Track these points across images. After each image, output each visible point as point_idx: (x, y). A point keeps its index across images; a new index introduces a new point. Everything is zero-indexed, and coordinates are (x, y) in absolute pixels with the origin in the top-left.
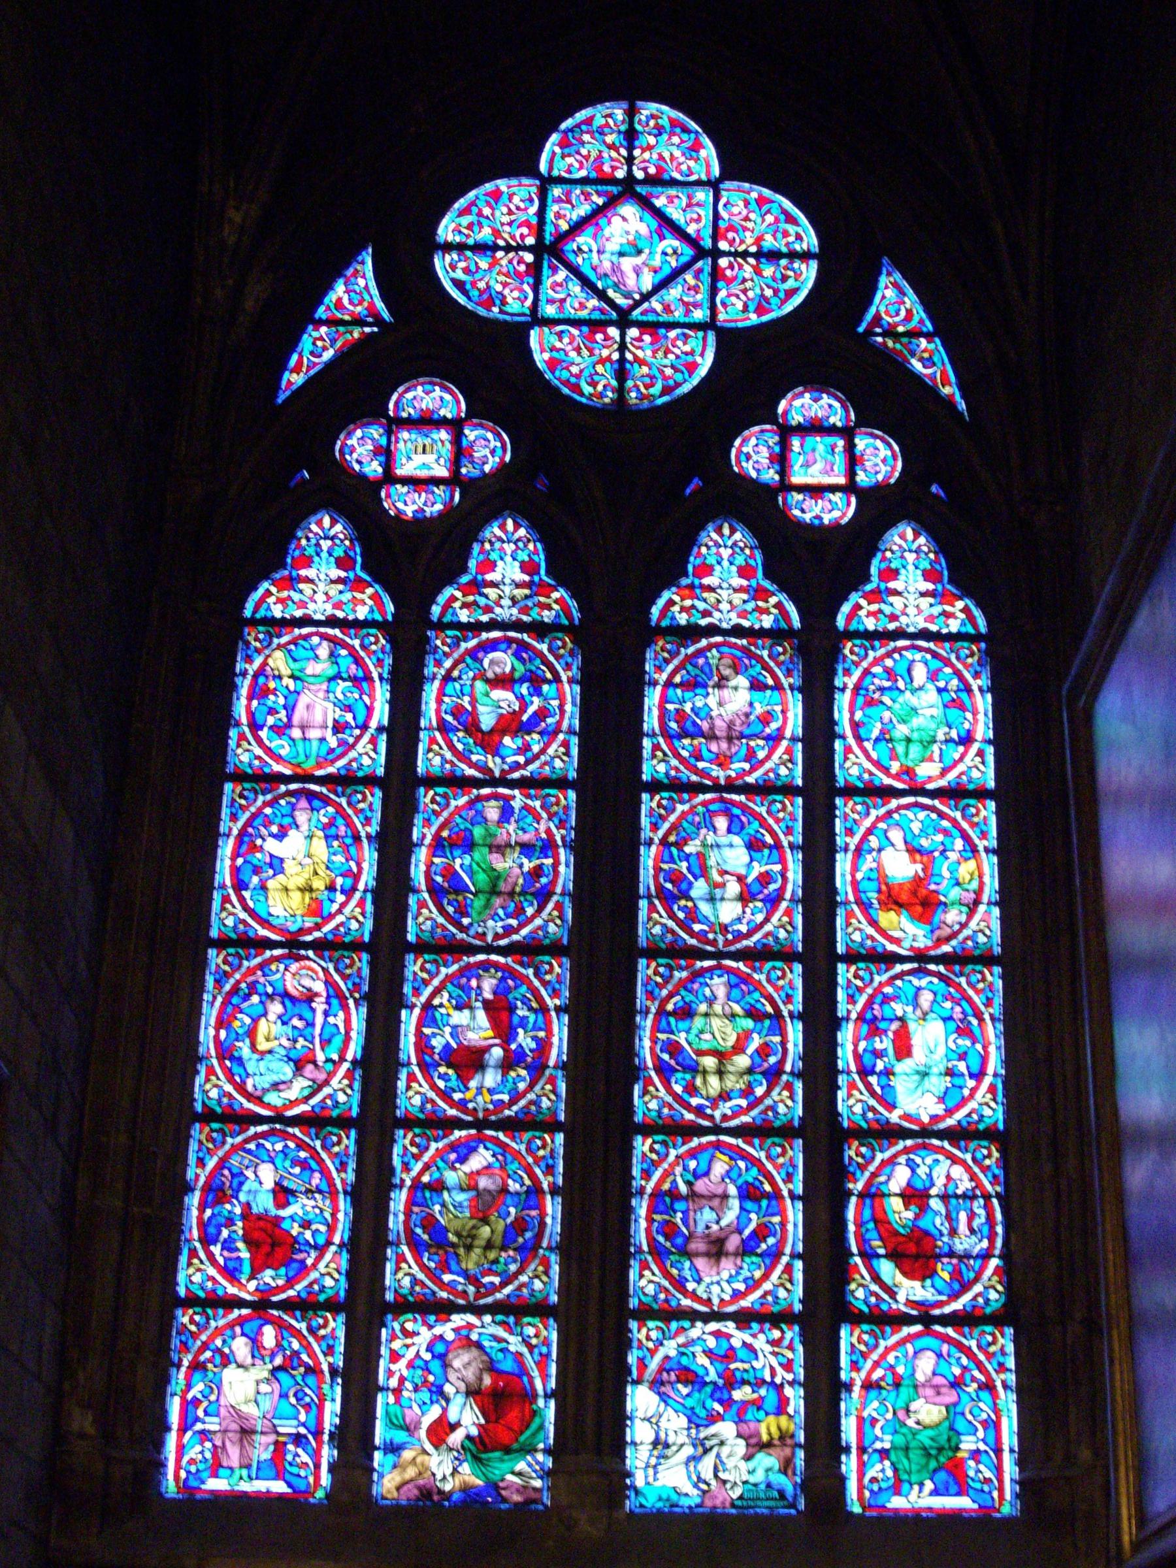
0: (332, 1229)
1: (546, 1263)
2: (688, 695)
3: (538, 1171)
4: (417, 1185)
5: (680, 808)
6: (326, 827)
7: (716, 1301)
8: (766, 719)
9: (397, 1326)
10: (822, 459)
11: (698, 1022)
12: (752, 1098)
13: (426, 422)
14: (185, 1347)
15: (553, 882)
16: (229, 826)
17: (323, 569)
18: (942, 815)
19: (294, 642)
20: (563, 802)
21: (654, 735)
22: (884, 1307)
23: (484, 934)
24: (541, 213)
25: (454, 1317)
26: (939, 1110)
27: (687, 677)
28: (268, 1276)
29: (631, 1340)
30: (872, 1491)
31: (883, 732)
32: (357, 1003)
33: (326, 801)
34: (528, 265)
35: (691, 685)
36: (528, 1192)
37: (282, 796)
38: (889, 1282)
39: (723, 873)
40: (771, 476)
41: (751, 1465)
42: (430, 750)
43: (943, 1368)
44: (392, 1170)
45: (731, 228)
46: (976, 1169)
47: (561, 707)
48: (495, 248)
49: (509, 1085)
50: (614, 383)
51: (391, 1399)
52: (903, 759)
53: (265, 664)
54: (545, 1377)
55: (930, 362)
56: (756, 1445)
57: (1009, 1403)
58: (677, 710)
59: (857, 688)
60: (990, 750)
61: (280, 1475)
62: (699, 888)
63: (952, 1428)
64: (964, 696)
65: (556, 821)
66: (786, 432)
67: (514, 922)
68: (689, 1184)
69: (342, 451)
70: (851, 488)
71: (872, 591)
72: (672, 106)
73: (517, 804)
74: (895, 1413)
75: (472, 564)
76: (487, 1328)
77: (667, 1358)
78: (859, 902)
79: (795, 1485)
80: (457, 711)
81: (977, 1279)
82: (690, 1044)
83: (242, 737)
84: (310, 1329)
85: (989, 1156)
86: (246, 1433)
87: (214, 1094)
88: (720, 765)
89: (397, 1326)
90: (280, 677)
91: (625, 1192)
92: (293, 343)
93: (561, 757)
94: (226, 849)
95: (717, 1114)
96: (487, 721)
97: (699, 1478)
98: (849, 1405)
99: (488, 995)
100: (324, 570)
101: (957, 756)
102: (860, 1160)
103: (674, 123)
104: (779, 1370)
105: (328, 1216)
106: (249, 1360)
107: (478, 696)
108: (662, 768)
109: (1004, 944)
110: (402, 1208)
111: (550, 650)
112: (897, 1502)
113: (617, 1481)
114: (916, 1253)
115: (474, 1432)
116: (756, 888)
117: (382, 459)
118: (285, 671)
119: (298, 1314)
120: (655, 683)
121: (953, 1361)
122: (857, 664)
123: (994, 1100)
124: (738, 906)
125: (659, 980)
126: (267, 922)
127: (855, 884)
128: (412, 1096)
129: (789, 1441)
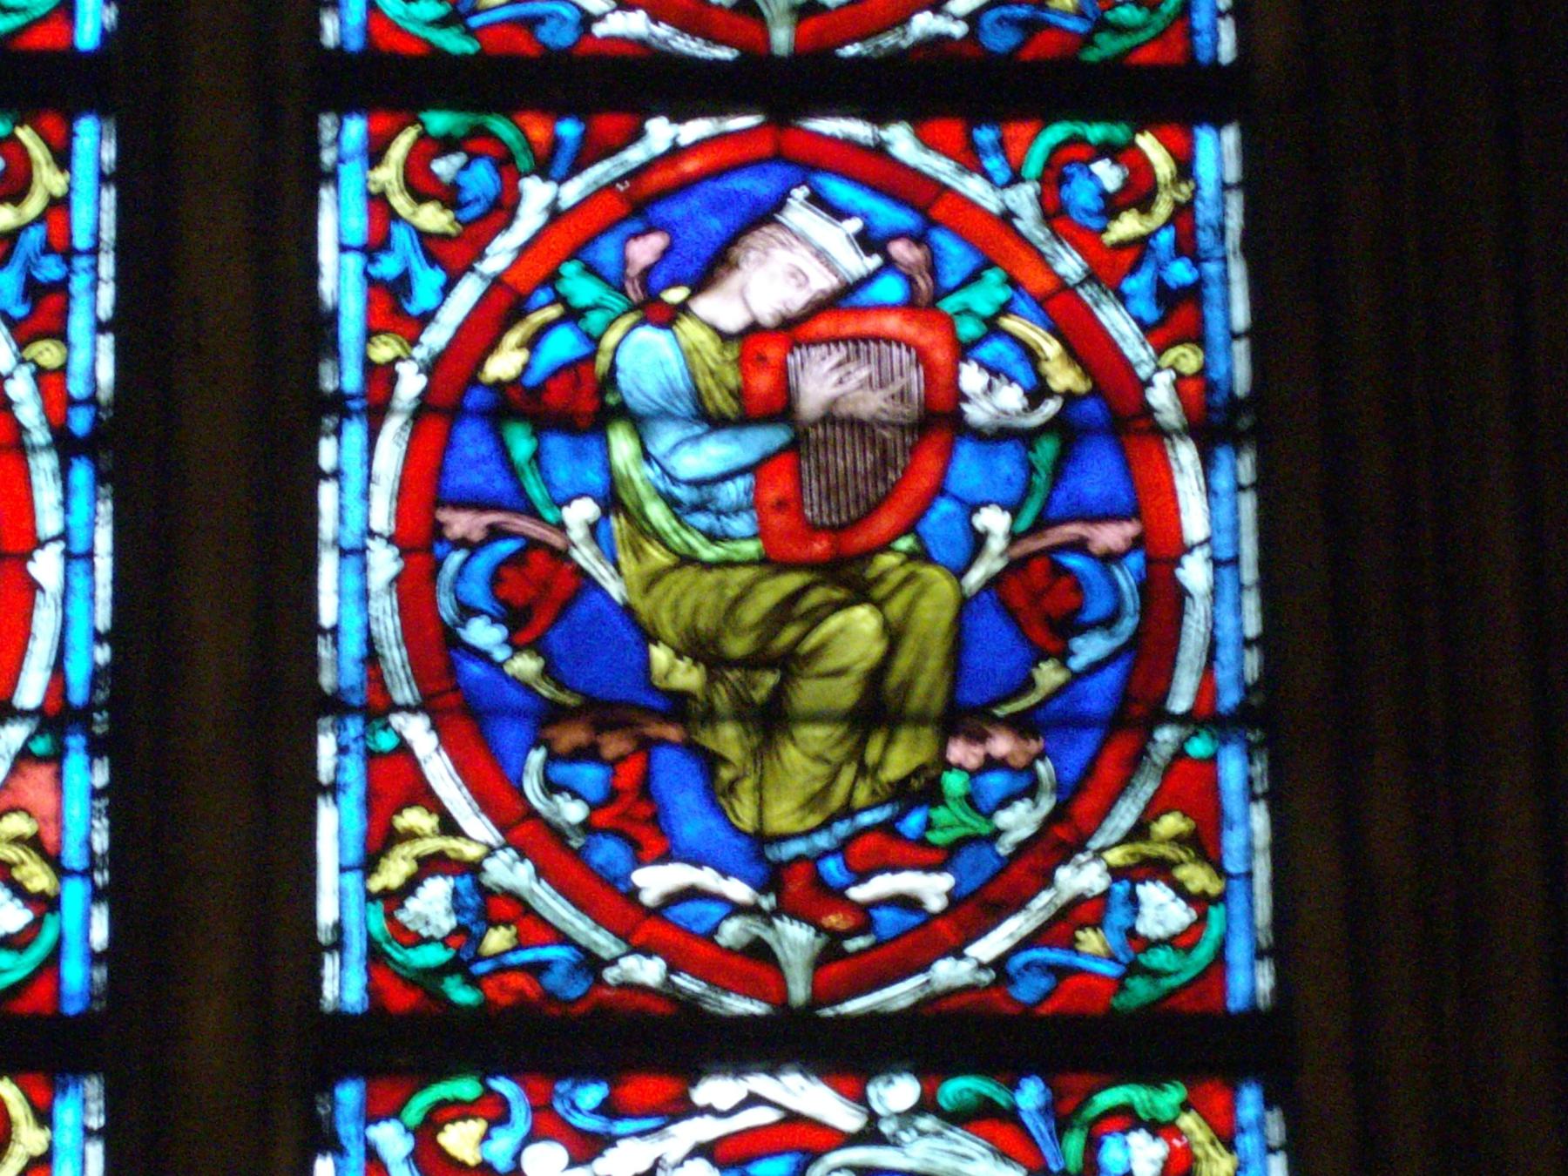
1: (1192, 789)
4: (455, 394)
9: (393, 1140)
25: (716, 1090)
44: (320, 328)
110: (382, 516)
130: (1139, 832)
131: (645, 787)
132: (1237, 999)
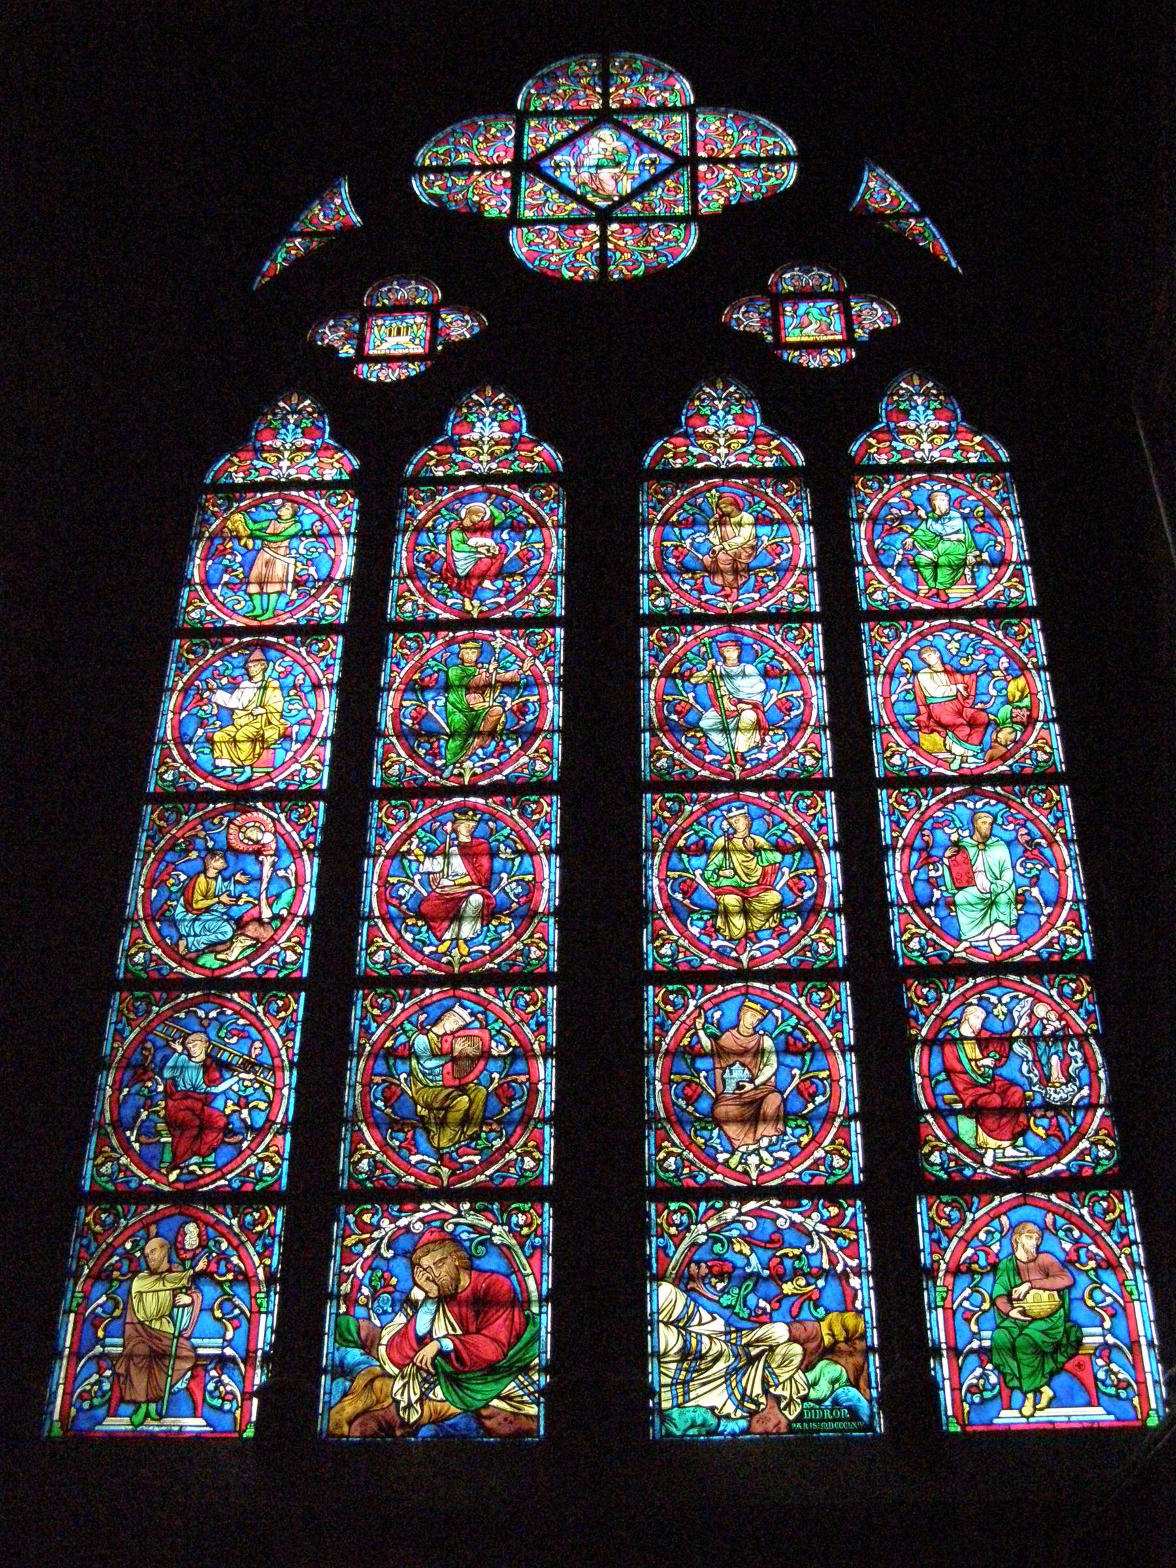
2: (686, 532)
3: (526, 1029)
7: (754, 1175)
8: (776, 549)
9: (351, 1218)
11: (718, 859)
12: (785, 938)
16: (175, 680)
18: (980, 634)
21: (653, 572)
22: (968, 1172)
23: (461, 775)
25: (425, 1206)
27: (684, 515)
29: (648, 1227)
30: (972, 1404)
33: (283, 651)
34: (505, 180)
36: (514, 1057)
37: (236, 648)
38: (971, 1142)
41: (811, 1376)
43: (1050, 1243)
44: (350, 1035)
49: (491, 935)
60: (1027, 571)
62: (710, 719)
63: (1067, 1318)
65: (543, 658)
68: (714, 1037)
73: (497, 644)
74: (993, 1303)
76: (465, 1219)
77: (694, 1245)
78: (895, 725)
79: (870, 1401)
81: (1080, 1135)
82: (707, 882)
88: (727, 596)
89: (351, 1218)
90: (239, 538)
94: (171, 703)
95: (744, 958)
96: (463, 565)
97: (744, 1395)
99: (464, 839)
104: (840, 1255)
105: (269, 1090)
106: (165, 1266)
108: (661, 602)
109: (1068, 761)
111: (532, 497)
112: (1008, 1418)
114: (1004, 1110)
116: (775, 715)
117: (355, 342)
120: (650, 524)
124: (757, 737)
126: (212, 774)
128: (379, 948)
129: (860, 1345)
130: (525, 1145)
131: (413, 1138)
132: (546, 1182)
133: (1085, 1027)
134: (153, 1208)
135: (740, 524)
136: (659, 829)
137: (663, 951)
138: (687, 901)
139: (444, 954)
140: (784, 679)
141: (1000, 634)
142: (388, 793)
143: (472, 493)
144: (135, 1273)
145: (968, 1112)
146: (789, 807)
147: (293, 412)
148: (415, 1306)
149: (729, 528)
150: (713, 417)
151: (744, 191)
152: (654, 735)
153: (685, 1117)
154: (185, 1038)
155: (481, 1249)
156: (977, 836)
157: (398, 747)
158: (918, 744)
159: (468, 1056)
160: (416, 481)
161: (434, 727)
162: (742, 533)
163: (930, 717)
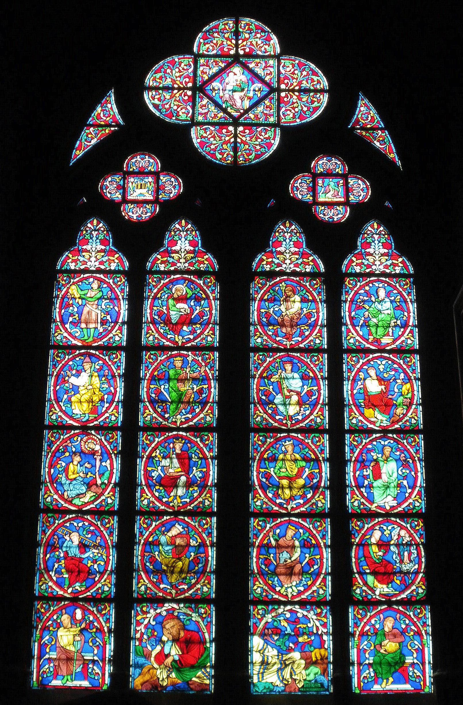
0: (107, 563)
2: (271, 305)
3: (204, 535)
5: (268, 360)
6: (99, 370)
8: (309, 316)
9: (139, 609)
10: (332, 190)
11: (279, 464)
12: (305, 499)
13: (141, 173)
14: (39, 619)
15: (209, 396)
17: (94, 245)
18: (394, 362)
19: (81, 281)
20: (212, 357)
22: (369, 597)
23: (176, 422)
24: (195, 71)
25: (166, 605)
26: (395, 503)
28: (77, 586)
29: (250, 614)
30: (364, 683)
31: (365, 322)
32: (116, 455)
34: (189, 97)
35: (272, 300)
36: (199, 546)
38: (372, 586)
39: (290, 391)
40: (309, 198)
41: (308, 672)
42: (147, 333)
45: (286, 78)
46: (412, 532)
47: (210, 311)
48: (173, 89)
50: (232, 153)
51: (137, 643)
52: (374, 335)
53: (67, 292)
54: (210, 633)
55: (383, 142)
56: (309, 663)
57: (428, 641)
58: (266, 312)
59: (352, 301)
61: (86, 678)
62: (279, 399)
64: (404, 305)
65: (209, 366)
66: (315, 176)
67: (190, 416)
68: (276, 540)
69: (101, 188)
70: (346, 203)
71: (358, 253)
72: (257, 20)
73: (190, 359)
74: (375, 647)
75: (166, 242)
77: (267, 623)
80: (160, 314)
81: (413, 583)
82: (276, 474)
83: (57, 327)
84: (98, 610)
85: (418, 525)
86: (69, 659)
87: (49, 500)
88: (287, 339)
89: (139, 609)
90: (75, 299)
91: (246, 545)
92: (77, 136)
93: (212, 337)
94: (51, 381)
95: (289, 507)
97: (283, 678)
98: (353, 643)
99: (178, 451)
100: (94, 245)
101: (400, 333)
102: (357, 528)
103: (257, 28)
104: (320, 627)
105: (104, 557)
106: (70, 626)
107: (170, 306)
108: (259, 340)
112: (376, 687)
113: (246, 680)
114: (384, 572)
115: (177, 658)
116: (306, 398)
117: (121, 191)
118: (77, 296)
119: (92, 604)
121: (402, 622)
122: (352, 289)
123: (420, 498)
124: (298, 408)
125: (260, 443)
127: (352, 395)
128: (145, 499)
130: (204, 582)
131: (161, 578)
133: (419, 541)
134: (63, 603)
135: (294, 302)
136: (257, 449)
137: (257, 504)
138: (267, 482)
139: (171, 502)
140: (310, 381)
141: (401, 362)
142: (146, 429)
143: (177, 279)
144: (59, 628)
145: (371, 573)
146: (310, 441)
147: (95, 230)
148: (164, 643)
149: (289, 303)
150: (284, 243)
151: (302, 110)
152: (255, 406)
153: (264, 572)
154: (70, 534)
155: (188, 622)
156: (384, 457)
157: (150, 407)
158: (363, 414)
159: (181, 546)
160: (152, 273)
161: (164, 399)
162: (295, 306)
163: (369, 401)
